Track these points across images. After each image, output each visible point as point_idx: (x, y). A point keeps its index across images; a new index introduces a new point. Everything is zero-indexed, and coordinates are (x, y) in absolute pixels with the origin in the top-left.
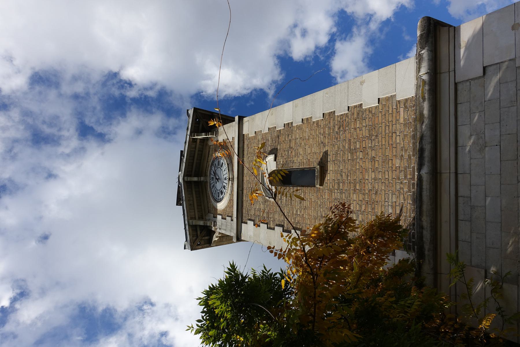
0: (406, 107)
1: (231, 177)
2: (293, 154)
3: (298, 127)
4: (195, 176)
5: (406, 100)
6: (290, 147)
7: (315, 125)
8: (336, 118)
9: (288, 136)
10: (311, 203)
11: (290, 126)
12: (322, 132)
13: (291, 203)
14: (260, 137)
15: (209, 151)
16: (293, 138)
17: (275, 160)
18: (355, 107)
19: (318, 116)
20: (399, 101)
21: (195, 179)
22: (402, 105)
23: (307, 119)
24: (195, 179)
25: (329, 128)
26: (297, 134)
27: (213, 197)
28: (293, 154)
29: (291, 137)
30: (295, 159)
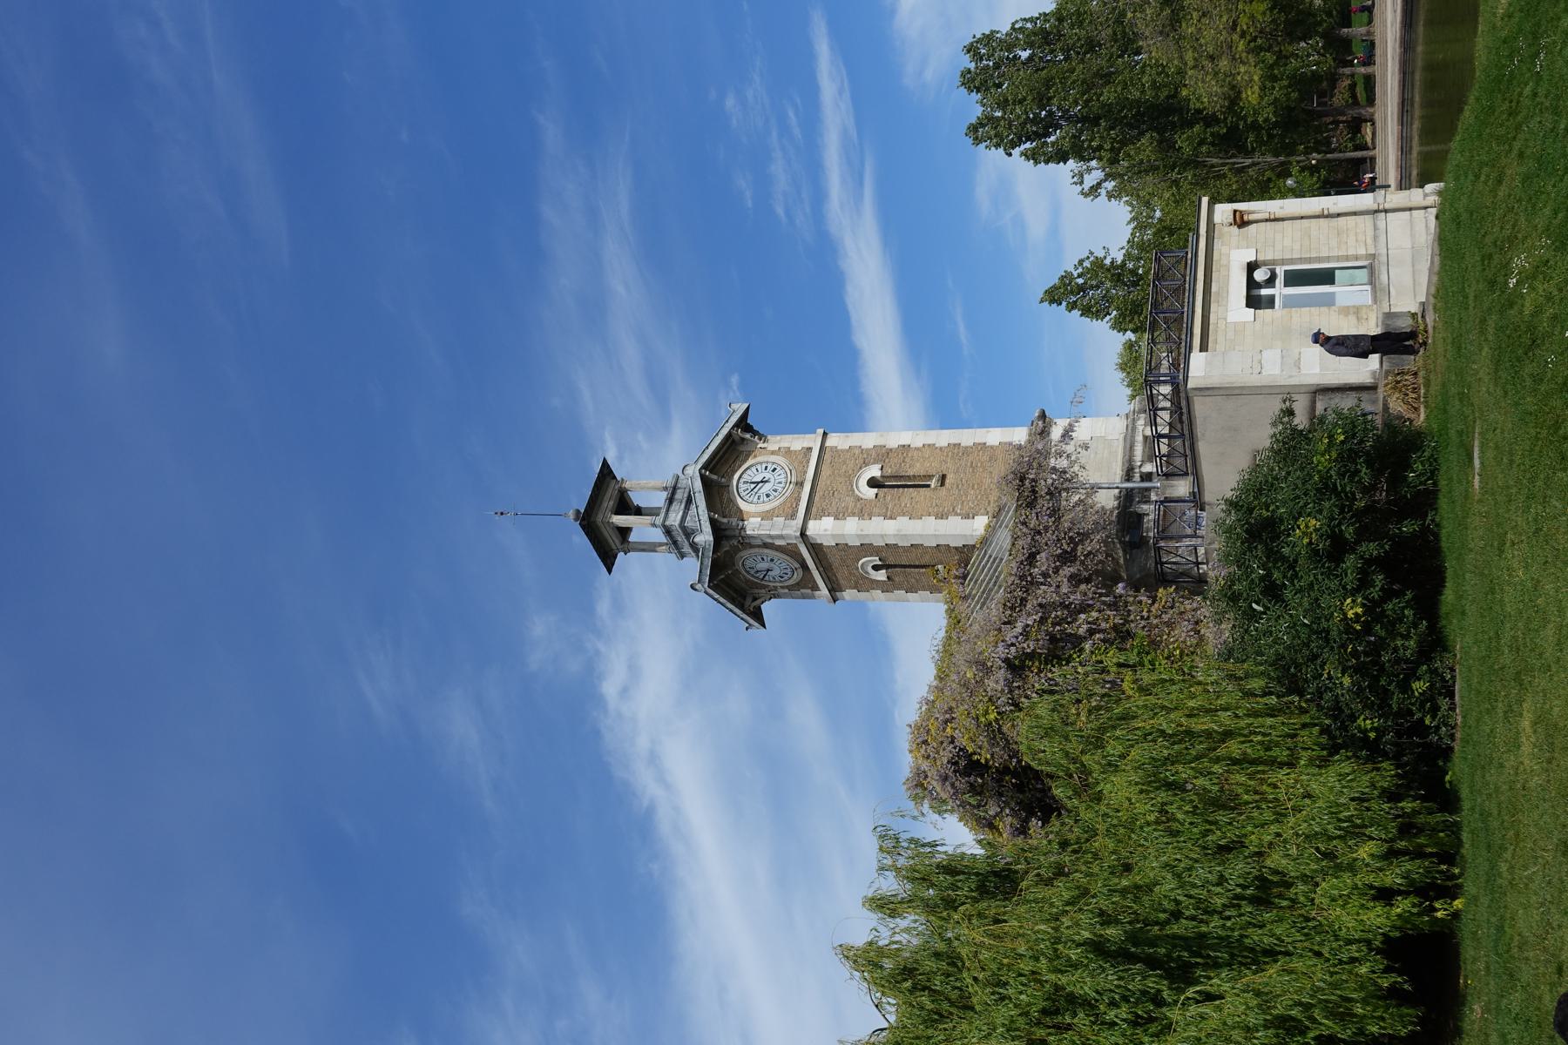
12: (945, 454)
15: (737, 457)
19: (944, 443)
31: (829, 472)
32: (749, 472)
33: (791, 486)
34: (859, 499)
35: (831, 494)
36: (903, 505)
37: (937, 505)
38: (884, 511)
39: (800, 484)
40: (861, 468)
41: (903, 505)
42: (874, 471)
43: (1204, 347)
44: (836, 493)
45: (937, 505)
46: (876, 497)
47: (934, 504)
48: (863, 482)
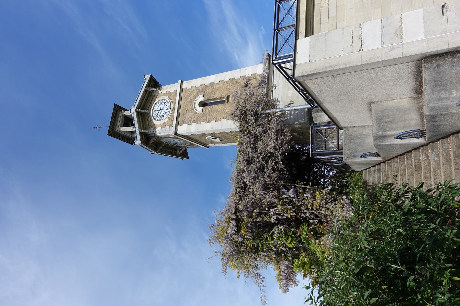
0: (260, 77)
1: (171, 107)
2: (214, 93)
3: (217, 84)
4: (142, 109)
5: (260, 75)
6: (212, 91)
7: (226, 83)
8: (235, 80)
9: (212, 87)
10: (221, 110)
11: (213, 83)
12: (229, 85)
13: (211, 111)
14: (194, 89)
16: (214, 87)
17: (204, 97)
18: (243, 77)
20: (258, 75)
21: (143, 111)
22: (259, 76)
23: (222, 81)
24: (143, 111)
25: (232, 83)
26: (217, 86)
27: (154, 119)
28: (214, 93)
29: (213, 87)
30: (214, 95)
31: (184, 101)
32: (156, 105)
33: (171, 110)
34: (196, 113)
35: (185, 112)
36: (213, 114)
37: (226, 113)
38: (206, 118)
39: (174, 108)
40: (196, 97)
41: (213, 114)
42: (201, 98)
43: (309, 32)
44: (187, 111)
45: (226, 113)
46: (202, 112)
47: (225, 112)
48: (197, 104)
